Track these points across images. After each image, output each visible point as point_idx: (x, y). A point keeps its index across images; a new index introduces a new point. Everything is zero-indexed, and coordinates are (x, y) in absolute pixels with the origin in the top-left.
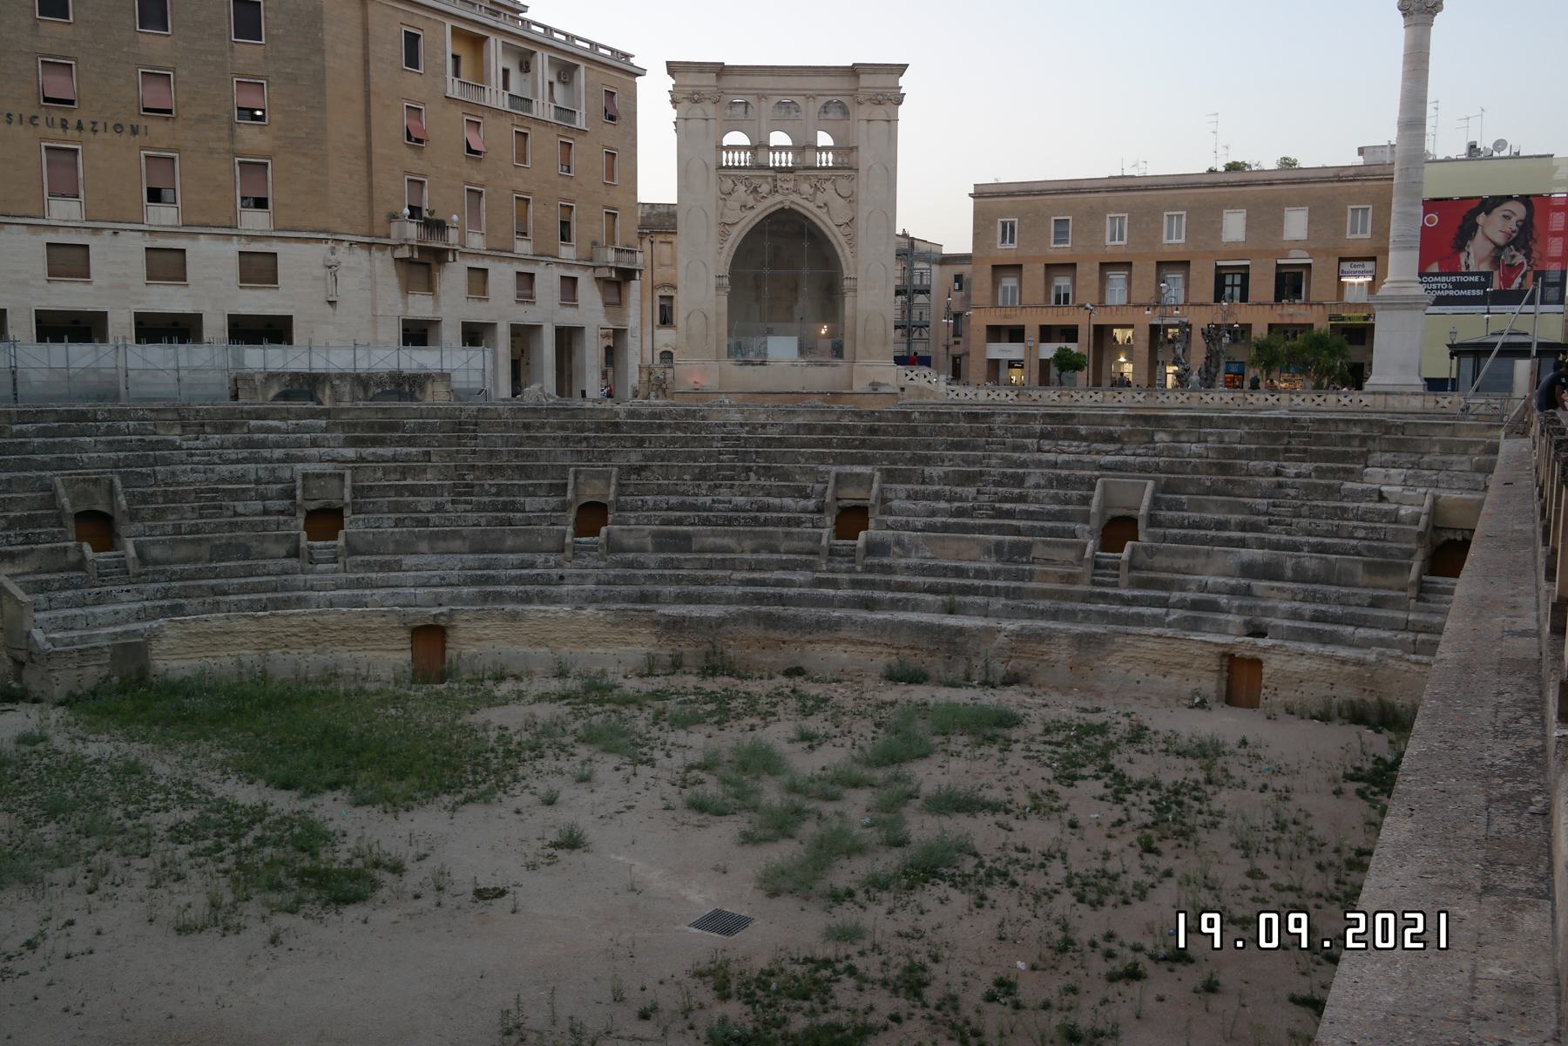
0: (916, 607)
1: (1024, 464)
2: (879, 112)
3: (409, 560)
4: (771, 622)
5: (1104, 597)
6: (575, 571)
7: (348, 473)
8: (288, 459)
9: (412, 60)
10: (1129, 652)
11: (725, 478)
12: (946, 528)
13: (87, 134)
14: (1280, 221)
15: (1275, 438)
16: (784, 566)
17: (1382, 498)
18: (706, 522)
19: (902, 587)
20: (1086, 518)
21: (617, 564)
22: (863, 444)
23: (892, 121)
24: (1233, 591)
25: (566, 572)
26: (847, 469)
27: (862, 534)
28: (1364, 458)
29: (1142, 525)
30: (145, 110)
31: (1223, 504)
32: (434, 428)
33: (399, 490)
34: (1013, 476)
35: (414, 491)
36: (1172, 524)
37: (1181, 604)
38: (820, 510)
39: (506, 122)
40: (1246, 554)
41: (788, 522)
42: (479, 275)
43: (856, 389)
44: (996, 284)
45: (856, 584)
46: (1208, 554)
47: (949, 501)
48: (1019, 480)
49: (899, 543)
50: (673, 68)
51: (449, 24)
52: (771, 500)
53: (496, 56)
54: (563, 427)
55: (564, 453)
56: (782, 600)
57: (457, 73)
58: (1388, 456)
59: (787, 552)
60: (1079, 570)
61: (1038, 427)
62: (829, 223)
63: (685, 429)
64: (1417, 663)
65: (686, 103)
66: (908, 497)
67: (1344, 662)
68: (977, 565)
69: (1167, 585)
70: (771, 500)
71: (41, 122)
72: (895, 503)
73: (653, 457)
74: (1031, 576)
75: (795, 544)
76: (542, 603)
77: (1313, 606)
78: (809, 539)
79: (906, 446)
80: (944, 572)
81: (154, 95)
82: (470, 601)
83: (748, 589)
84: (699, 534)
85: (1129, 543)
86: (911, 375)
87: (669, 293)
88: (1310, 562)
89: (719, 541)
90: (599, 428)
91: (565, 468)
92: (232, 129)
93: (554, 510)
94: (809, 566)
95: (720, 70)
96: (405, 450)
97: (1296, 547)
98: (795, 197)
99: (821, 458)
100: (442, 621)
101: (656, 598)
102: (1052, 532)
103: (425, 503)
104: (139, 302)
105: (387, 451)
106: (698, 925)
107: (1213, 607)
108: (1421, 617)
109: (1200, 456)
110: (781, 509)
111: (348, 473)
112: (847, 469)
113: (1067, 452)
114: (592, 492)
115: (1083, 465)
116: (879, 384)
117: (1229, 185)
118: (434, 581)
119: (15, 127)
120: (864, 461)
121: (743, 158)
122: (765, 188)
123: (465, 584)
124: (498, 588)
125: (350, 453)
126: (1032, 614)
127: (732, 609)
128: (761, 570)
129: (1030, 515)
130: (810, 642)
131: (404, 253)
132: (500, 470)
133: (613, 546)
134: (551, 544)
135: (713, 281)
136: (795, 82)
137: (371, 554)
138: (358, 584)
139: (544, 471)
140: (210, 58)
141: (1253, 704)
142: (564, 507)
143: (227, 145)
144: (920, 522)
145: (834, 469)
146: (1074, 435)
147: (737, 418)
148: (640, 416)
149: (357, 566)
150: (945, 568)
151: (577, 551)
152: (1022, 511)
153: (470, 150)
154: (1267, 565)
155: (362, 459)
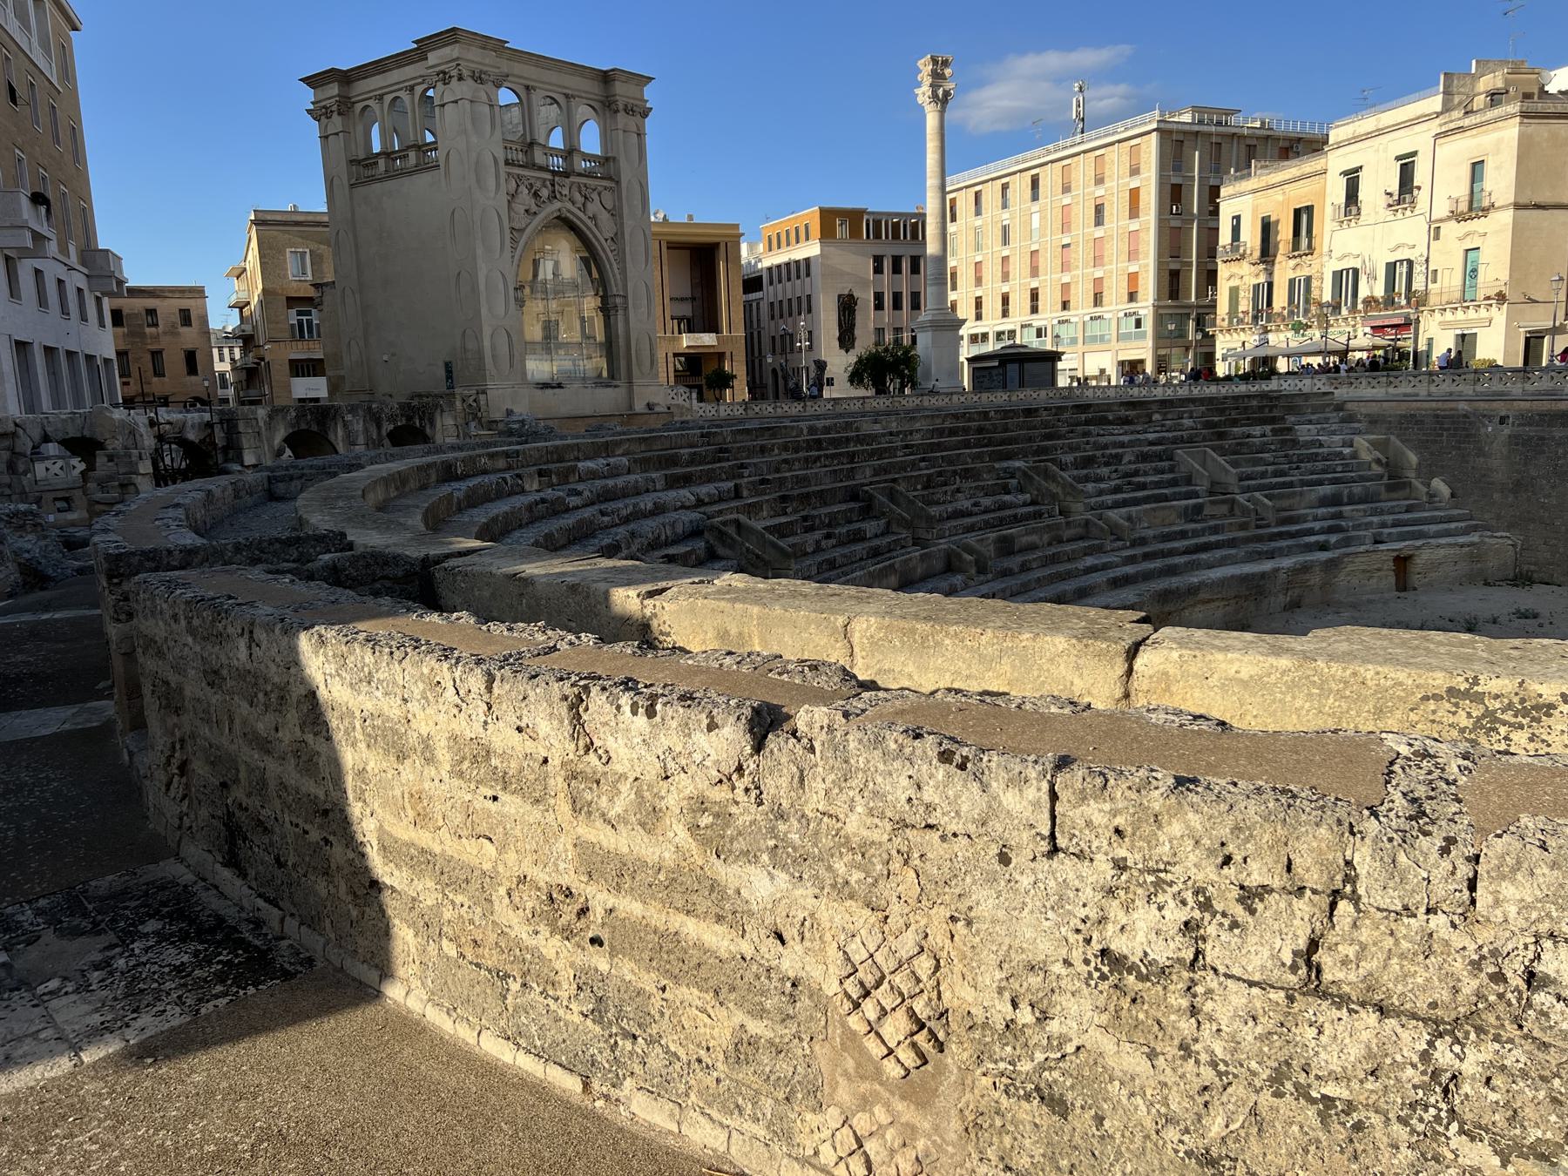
8: (659, 510)
17: (1321, 445)
23: (640, 135)
48: (1118, 458)
59: (1068, 541)
65: (470, 82)
88: (1357, 489)
93: (882, 534)
95: (498, 46)
98: (569, 206)
122: (545, 193)
134: (938, 565)
154: (1334, 495)
155: (700, 503)
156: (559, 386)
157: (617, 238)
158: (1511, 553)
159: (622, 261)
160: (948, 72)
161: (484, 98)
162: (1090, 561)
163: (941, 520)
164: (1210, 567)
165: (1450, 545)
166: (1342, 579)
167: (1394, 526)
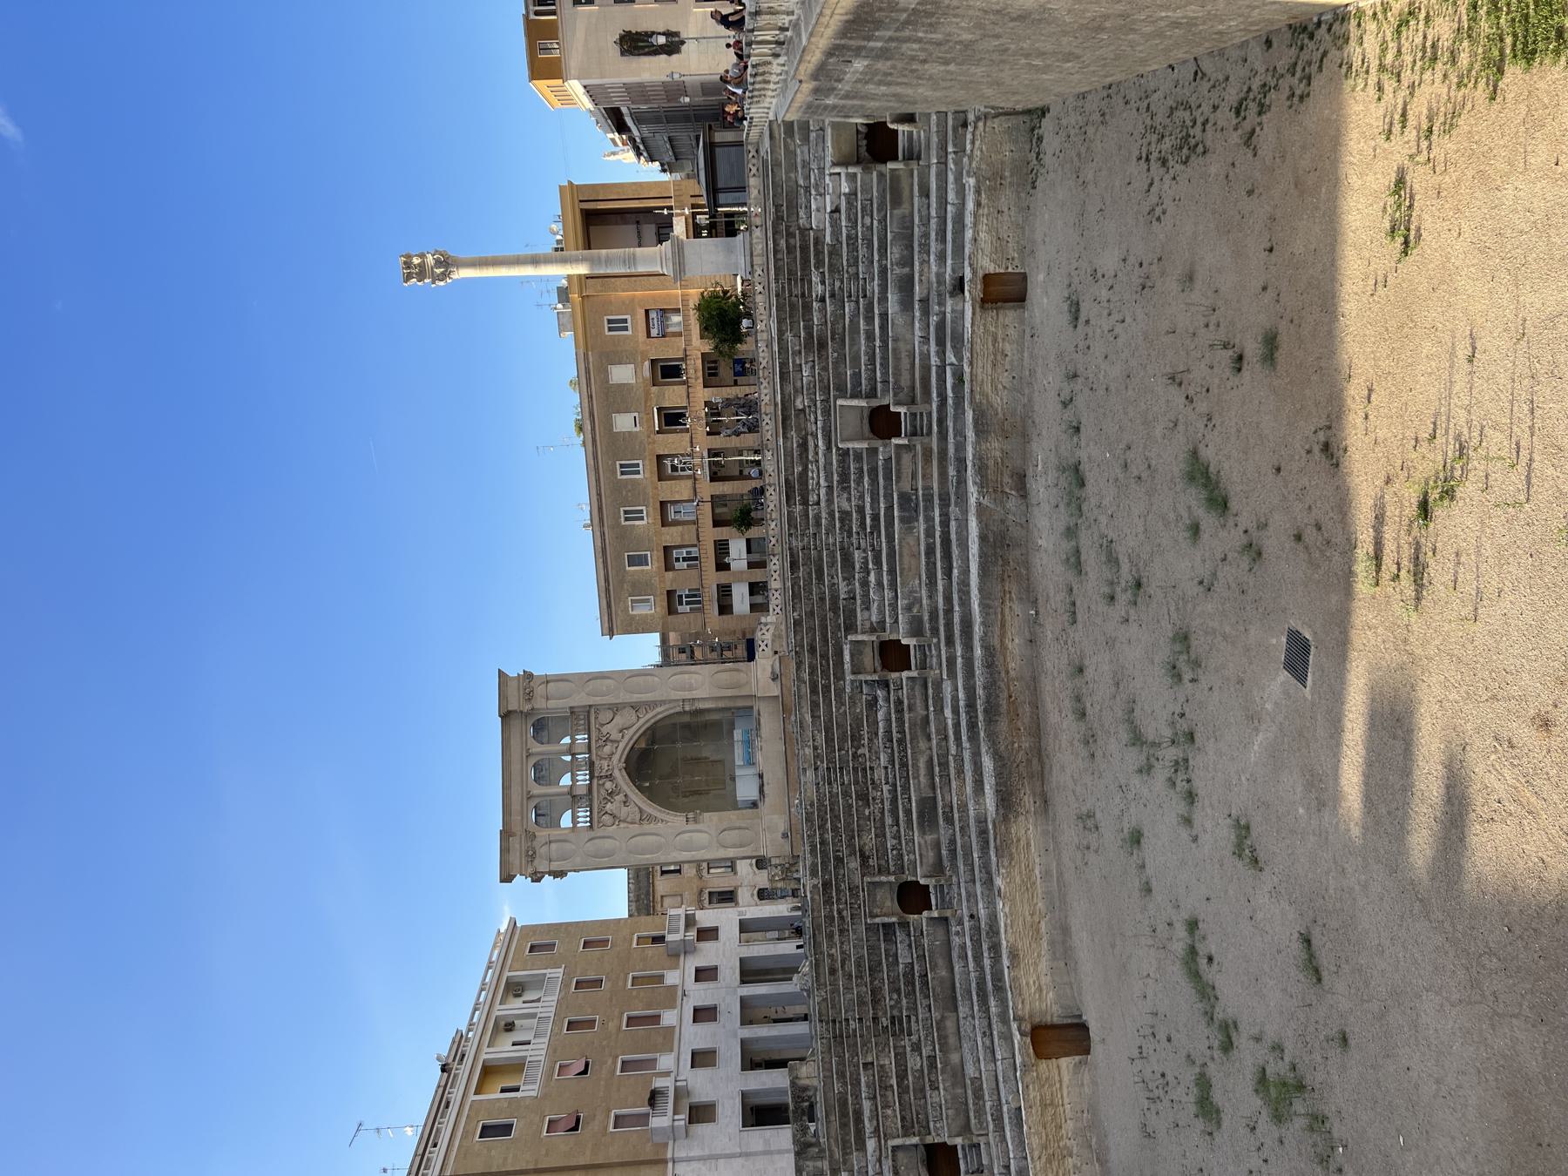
0: (964, 583)
1: (831, 514)
2: (540, 690)
3: (970, 1071)
4: (992, 711)
5: (942, 421)
6: (965, 904)
7: (891, 1143)
9: (505, 1129)
10: (988, 388)
11: (865, 776)
12: (892, 571)
14: (621, 386)
15: (793, 306)
16: (940, 710)
17: (837, 210)
18: (906, 789)
19: (948, 599)
20: (873, 452)
21: (954, 867)
22: (824, 656)
23: (547, 680)
24: (926, 312)
25: (966, 912)
26: (847, 667)
27: (904, 642)
28: (804, 231)
29: (875, 403)
31: (852, 340)
32: (841, 1063)
33: (903, 1090)
34: (842, 520)
35: (902, 1076)
36: (872, 379)
37: (942, 353)
38: (885, 684)
40: (893, 306)
41: (900, 711)
42: (697, 1059)
43: (777, 692)
44: (676, 523)
45: (950, 641)
46: (895, 340)
47: (868, 574)
48: (845, 515)
49: (909, 608)
50: (507, 878)
51: (472, 1097)
52: (881, 730)
53: (504, 1049)
54: (830, 936)
55: (855, 932)
56: (971, 706)
57: (517, 1089)
58: (802, 213)
60: (919, 447)
61: (799, 508)
63: (823, 820)
64: (973, 143)
65: (536, 862)
66: (868, 609)
67: (978, 204)
68: (922, 536)
69: (926, 368)
70: (881, 730)
72: (874, 619)
73: (851, 845)
74: (928, 488)
75: (919, 703)
76: (998, 933)
77: (933, 244)
78: (913, 689)
79: (823, 619)
80: (931, 566)
82: (1003, 1002)
83: (964, 738)
84: (918, 789)
85: (892, 409)
87: (706, 896)
88: (894, 253)
89: (922, 772)
90: (828, 902)
91: (869, 928)
94: (938, 685)
95: (506, 834)
96: (863, 1088)
97: (883, 271)
98: (615, 758)
99: (840, 692)
100: (1027, 1027)
101: (981, 821)
102: (888, 478)
103: (914, 1062)
105: (867, 1105)
106: (1302, 679)
107: (941, 326)
108: (934, 152)
109: (813, 367)
110: (888, 720)
111: (891, 1143)
112: (847, 667)
113: (818, 480)
114: (888, 901)
115: (828, 463)
116: (773, 672)
117: (593, 429)
118: (988, 1043)
120: (839, 653)
121: (583, 814)
123: (988, 1010)
124: (989, 977)
125: (871, 1144)
126: (961, 481)
127: (983, 750)
128: (945, 728)
129: (875, 500)
130: (1007, 672)
132: (875, 992)
133: (938, 869)
134: (940, 932)
135: (691, 826)
136: (516, 768)
137: (967, 1111)
138: (998, 1119)
139: (873, 949)
141: (1024, 277)
142: (904, 925)
144: (888, 594)
145: (849, 677)
146: (804, 474)
147: (810, 774)
148: (814, 865)
149: (980, 1123)
150: (927, 564)
151: (945, 903)
152: (872, 508)
153: (585, 1072)
155: (877, 1130)
156: (761, 776)
157: (635, 707)
158: (996, 123)
159: (655, 704)
160: (416, 261)
161: (545, 849)
162: (948, 713)
163: (897, 836)
164: (966, 571)
165: (975, 225)
166: (999, 401)
167: (944, 241)
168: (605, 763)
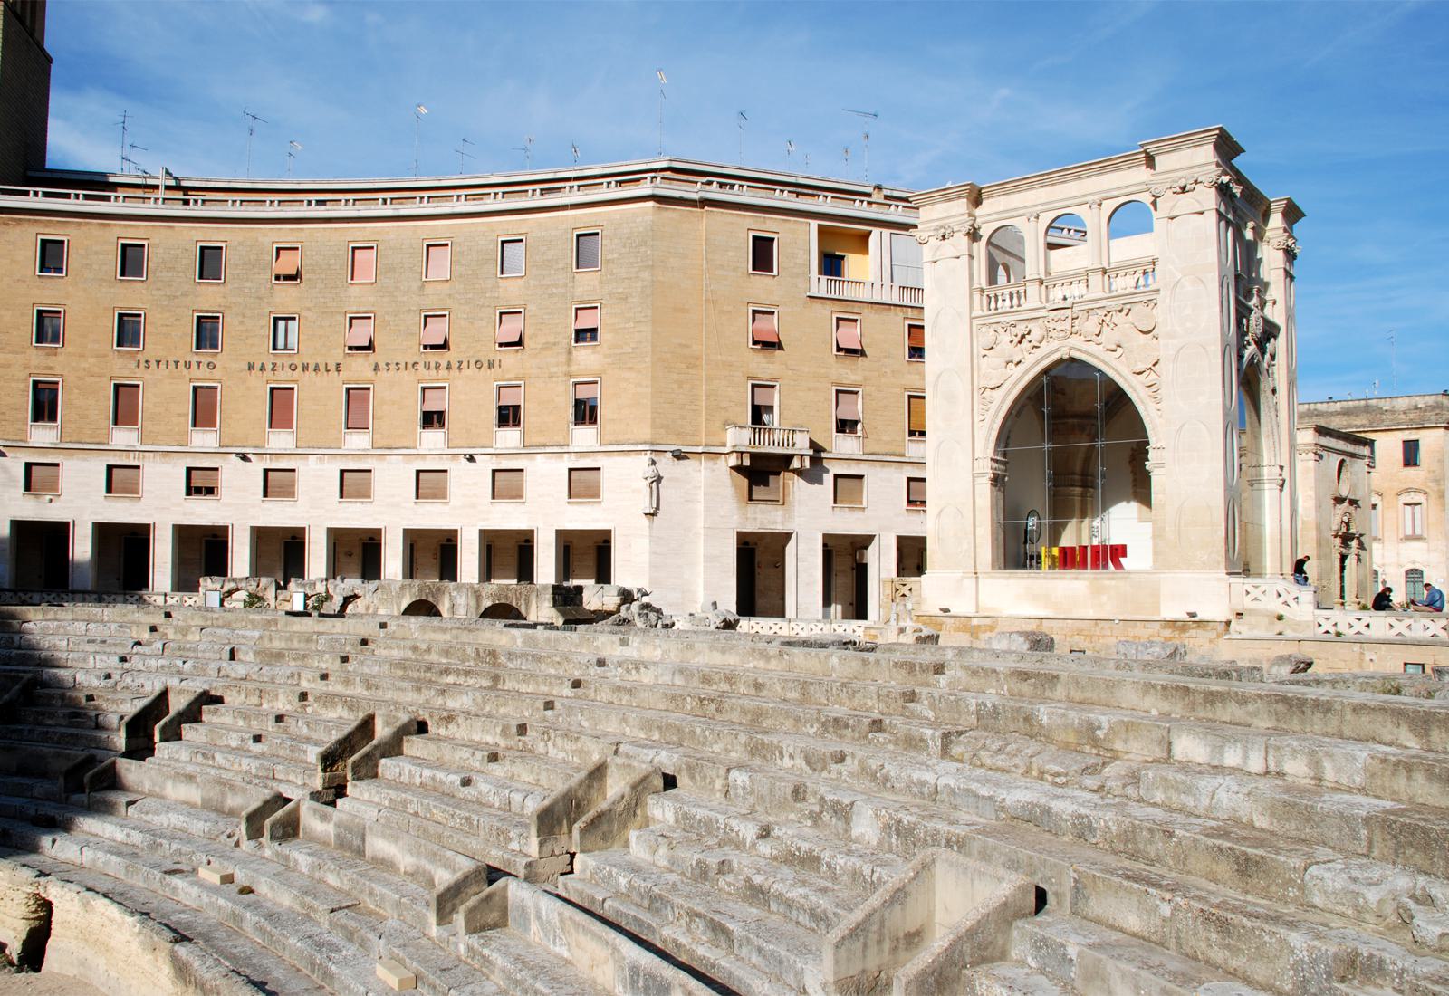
13: (455, 372)
30: (501, 345)
39: (900, 314)
51: (814, 224)
62: (1120, 371)
71: (420, 366)
81: (510, 330)
86: (1254, 593)
92: (570, 353)
98: (1074, 341)
104: (484, 520)
119: (403, 373)
122: (1036, 334)
131: (733, 461)
140: (555, 291)
143: (565, 368)
168: (1067, 325)
